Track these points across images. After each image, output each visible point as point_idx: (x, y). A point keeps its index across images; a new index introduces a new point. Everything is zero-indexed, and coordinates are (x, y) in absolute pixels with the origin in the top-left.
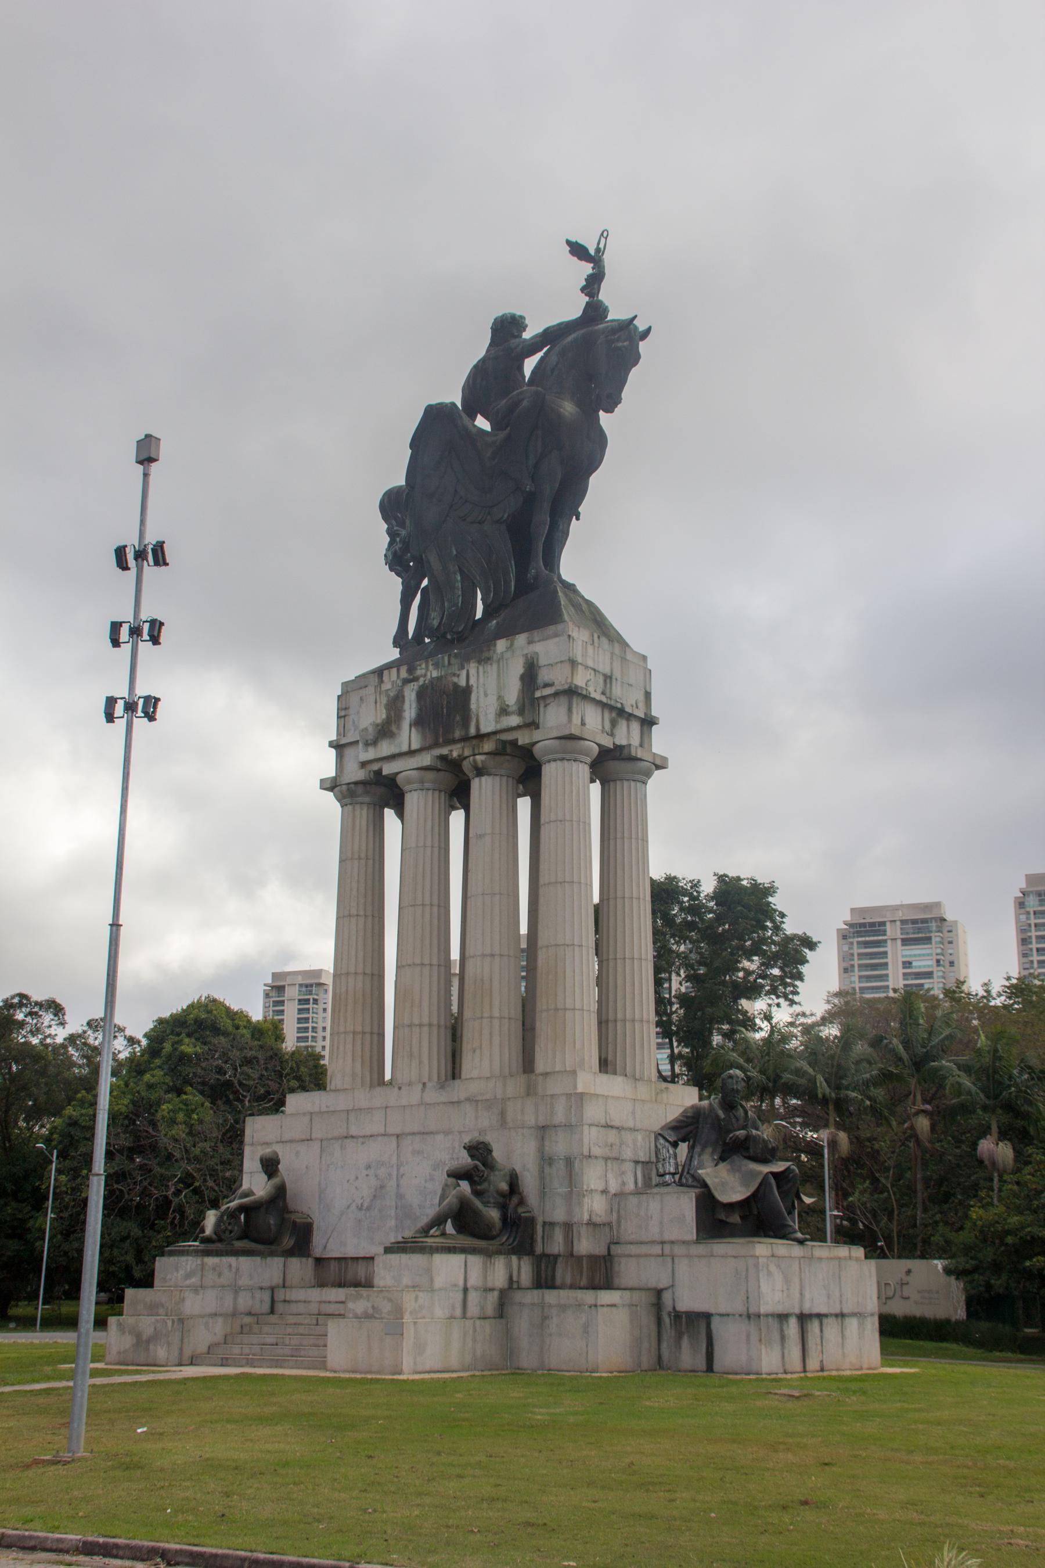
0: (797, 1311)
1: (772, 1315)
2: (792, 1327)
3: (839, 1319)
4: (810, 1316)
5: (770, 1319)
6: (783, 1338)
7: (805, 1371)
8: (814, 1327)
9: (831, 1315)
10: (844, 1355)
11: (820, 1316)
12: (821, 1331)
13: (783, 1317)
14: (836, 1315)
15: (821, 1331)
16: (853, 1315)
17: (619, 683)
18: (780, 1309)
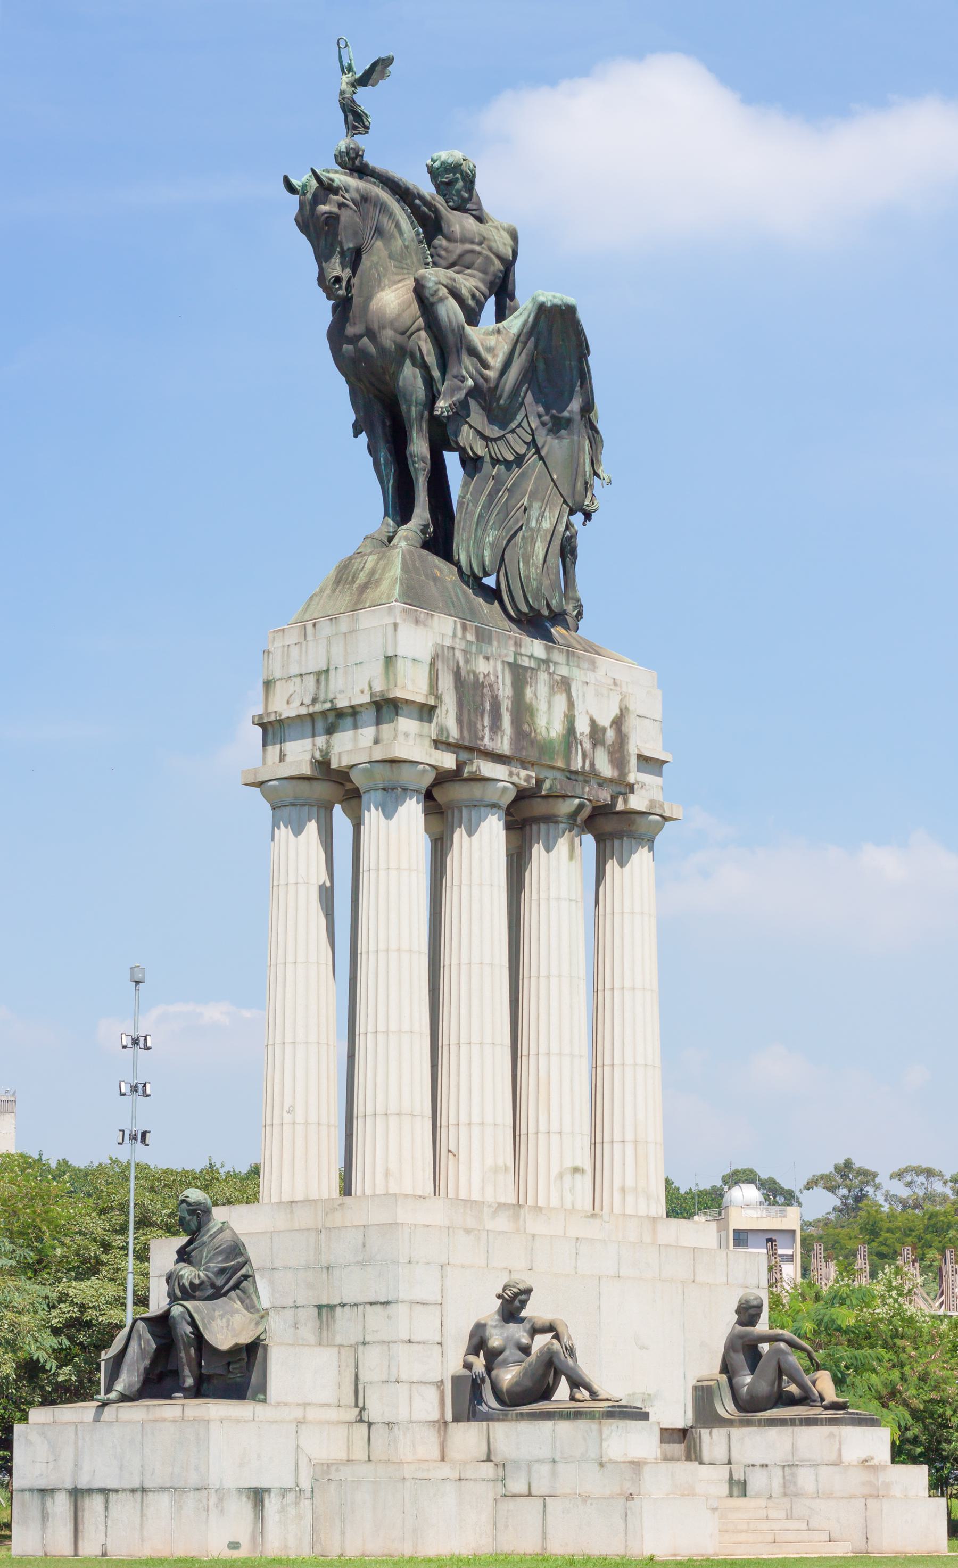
0: (69, 1485)
1: (31, 1490)
2: (61, 1505)
3: (138, 1495)
4: (90, 1491)
5: (27, 1494)
6: (45, 1516)
7: (76, 1555)
8: (94, 1504)
9: (124, 1490)
10: (142, 1539)
11: (104, 1491)
12: (106, 1508)
13: (45, 1492)
14: (133, 1491)
15: (106, 1508)
16: (163, 1489)
17: (340, 671)
18: (42, 1484)
